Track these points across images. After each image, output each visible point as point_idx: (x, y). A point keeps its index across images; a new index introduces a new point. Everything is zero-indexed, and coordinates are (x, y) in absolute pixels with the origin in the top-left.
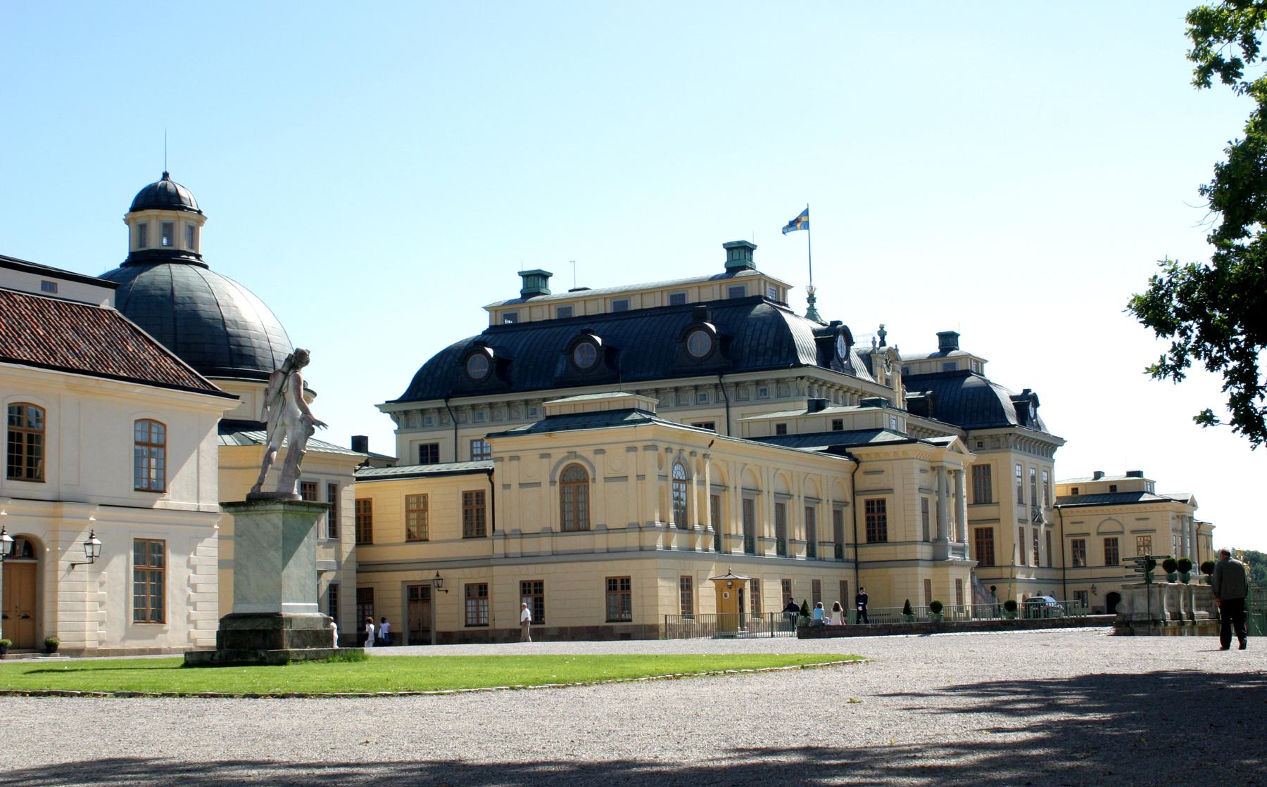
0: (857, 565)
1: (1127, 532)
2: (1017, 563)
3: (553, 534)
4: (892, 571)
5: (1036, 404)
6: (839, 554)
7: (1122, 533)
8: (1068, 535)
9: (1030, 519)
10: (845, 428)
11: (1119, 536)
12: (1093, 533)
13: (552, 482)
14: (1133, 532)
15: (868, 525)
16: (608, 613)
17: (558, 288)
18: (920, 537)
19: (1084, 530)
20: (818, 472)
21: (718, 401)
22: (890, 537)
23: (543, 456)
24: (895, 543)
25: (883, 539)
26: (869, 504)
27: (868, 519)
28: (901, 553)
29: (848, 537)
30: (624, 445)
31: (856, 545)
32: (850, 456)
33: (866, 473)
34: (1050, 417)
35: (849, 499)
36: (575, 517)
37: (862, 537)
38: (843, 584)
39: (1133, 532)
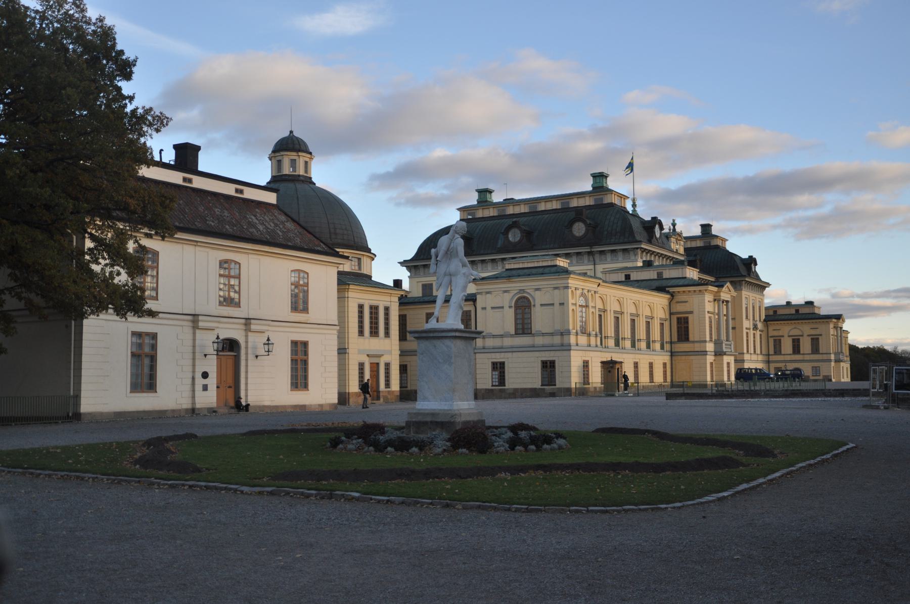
0: (672, 354)
1: (805, 335)
2: (745, 351)
3: (512, 336)
4: (692, 357)
5: (756, 264)
6: (662, 347)
9: (752, 327)
12: (786, 335)
13: (510, 307)
15: (678, 331)
16: (542, 381)
17: (497, 198)
18: (708, 339)
19: (780, 333)
20: (655, 304)
21: (589, 260)
22: (691, 338)
23: (505, 292)
24: (694, 342)
25: (687, 339)
26: (678, 319)
27: (678, 328)
28: (697, 347)
31: (671, 343)
32: (668, 292)
33: (678, 302)
34: (762, 271)
35: (668, 317)
36: (523, 327)
37: (675, 339)
38: (665, 364)
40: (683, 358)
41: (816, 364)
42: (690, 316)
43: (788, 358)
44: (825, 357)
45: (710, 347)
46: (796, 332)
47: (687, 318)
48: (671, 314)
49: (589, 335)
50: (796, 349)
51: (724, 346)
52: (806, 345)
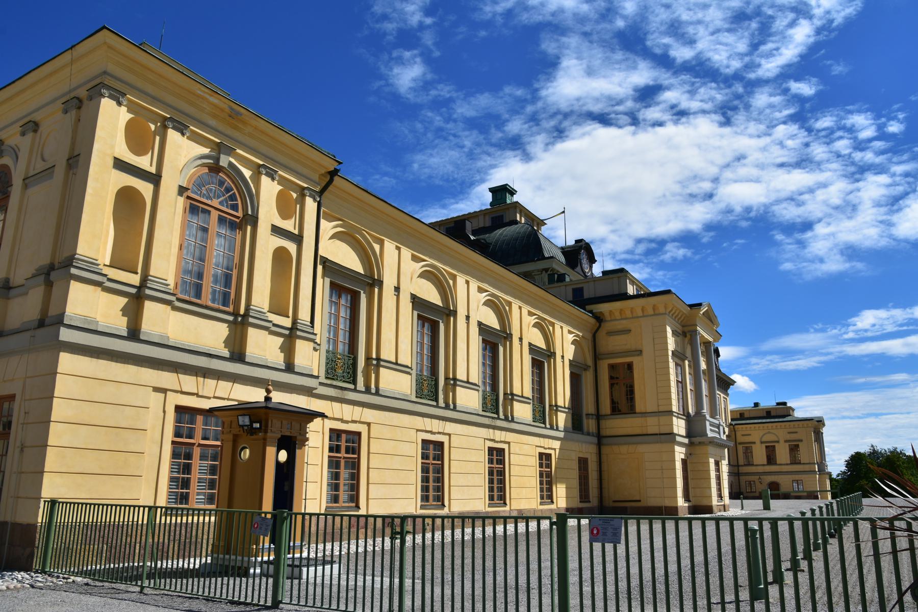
0: (600, 439)
1: (782, 441)
4: (642, 448)
7: (778, 442)
8: (740, 443)
10: (586, 296)
11: (776, 445)
14: (786, 441)
22: (639, 407)
28: (652, 425)
29: (589, 406)
30: (59, 105)
31: (598, 417)
35: (590, 362)
37: (606, 408)
38: (583, 463)
39: (786, 441)
40: (624, 449)
41: (797, 477)
42: (636, 361)
43: (760, 469)
44: (807, 468)
45: (679, 426)
46: (767, 438)
47: (630, 366)
48: (596, 357)
49: (240, 323)
50: (771, 459)
51: (708, 427)
52: (783, 454)
